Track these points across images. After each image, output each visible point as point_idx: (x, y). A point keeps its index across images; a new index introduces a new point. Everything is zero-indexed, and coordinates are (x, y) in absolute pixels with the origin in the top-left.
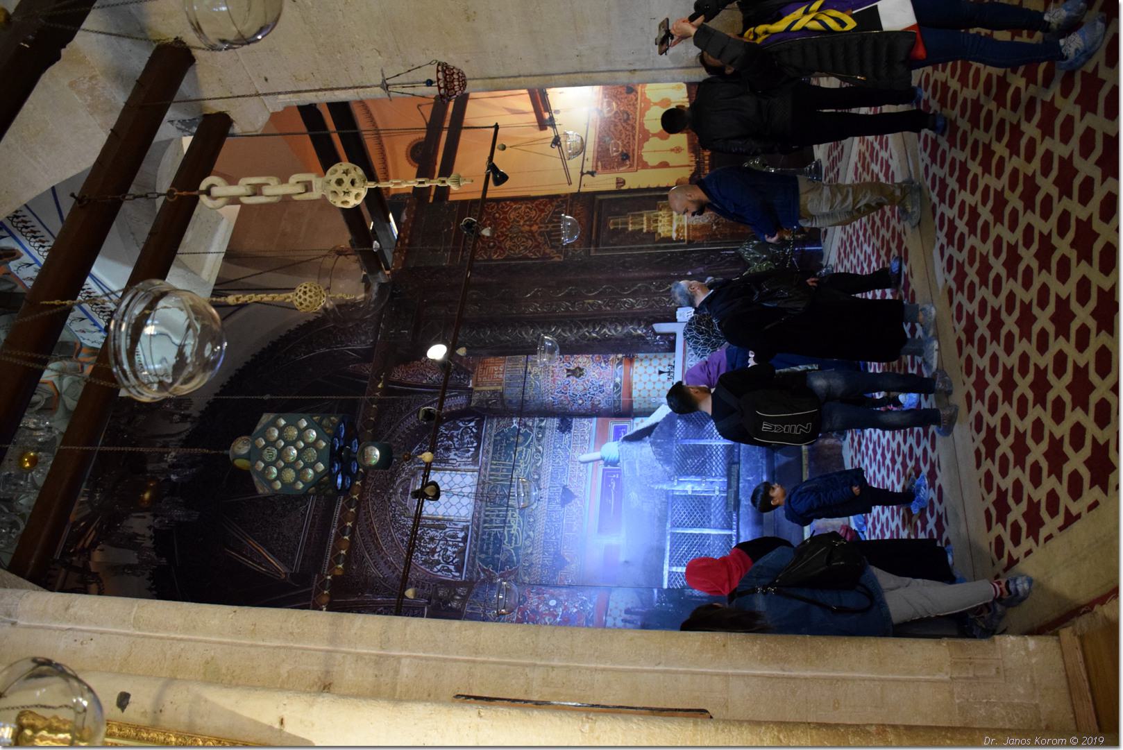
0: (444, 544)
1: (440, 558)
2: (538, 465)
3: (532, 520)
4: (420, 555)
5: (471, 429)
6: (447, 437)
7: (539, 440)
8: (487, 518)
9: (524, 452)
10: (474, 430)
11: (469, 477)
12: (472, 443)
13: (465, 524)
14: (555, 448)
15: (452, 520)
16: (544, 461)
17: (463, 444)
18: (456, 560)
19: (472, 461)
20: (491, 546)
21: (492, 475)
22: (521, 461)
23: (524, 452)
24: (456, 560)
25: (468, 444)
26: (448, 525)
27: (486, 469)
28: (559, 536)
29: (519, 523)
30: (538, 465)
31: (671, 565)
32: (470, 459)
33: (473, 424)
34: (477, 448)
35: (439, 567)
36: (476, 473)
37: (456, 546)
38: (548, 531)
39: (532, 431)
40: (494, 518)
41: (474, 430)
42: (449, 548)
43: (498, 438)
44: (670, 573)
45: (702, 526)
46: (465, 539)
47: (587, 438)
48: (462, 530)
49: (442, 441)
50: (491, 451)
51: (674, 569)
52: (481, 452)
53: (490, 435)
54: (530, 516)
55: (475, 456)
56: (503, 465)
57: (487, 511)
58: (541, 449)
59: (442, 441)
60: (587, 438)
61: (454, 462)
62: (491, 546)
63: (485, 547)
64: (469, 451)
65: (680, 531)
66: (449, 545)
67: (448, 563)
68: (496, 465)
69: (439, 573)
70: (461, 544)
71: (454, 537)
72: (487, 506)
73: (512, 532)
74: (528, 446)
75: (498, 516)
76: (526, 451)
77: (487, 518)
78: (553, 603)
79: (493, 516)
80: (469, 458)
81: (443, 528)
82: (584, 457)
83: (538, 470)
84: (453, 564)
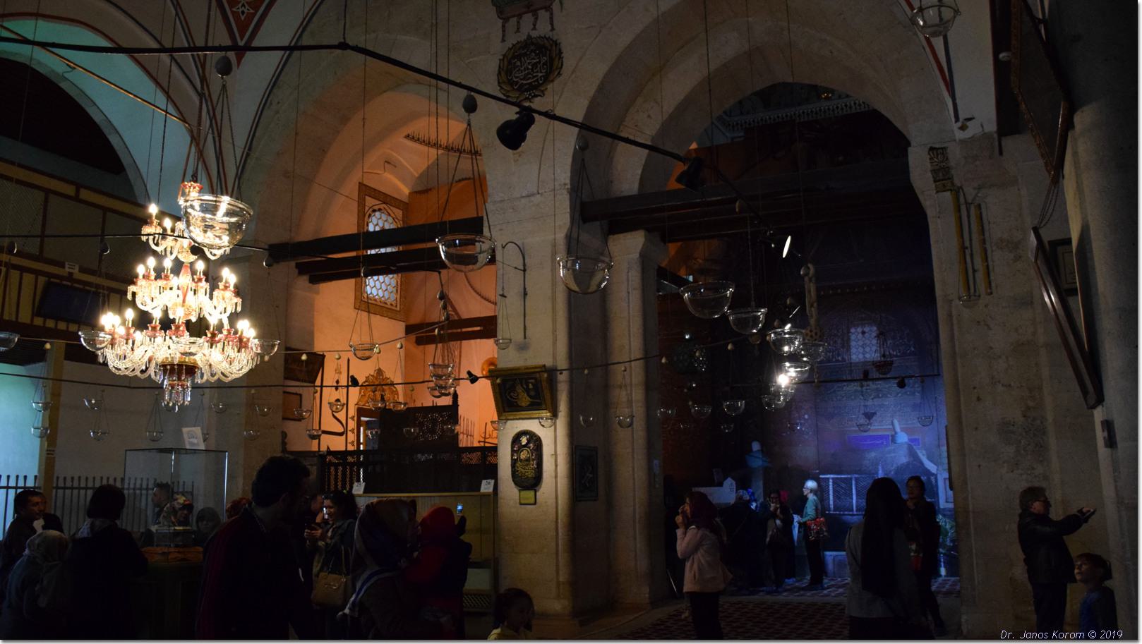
7: (906, 393)
30: (889, 395)
31: (833, 478)
33: (913, 349)
39: (912, 388)
41: (908, 352)
44: (828, 479)
45: (857, 495)
46: (838, 361)
48: (843, 358)
51: (831, 480)
65: (854, 482)
71: (839, 355)
78: (806, 417)
81: (843, 347)
82: (896, 422)
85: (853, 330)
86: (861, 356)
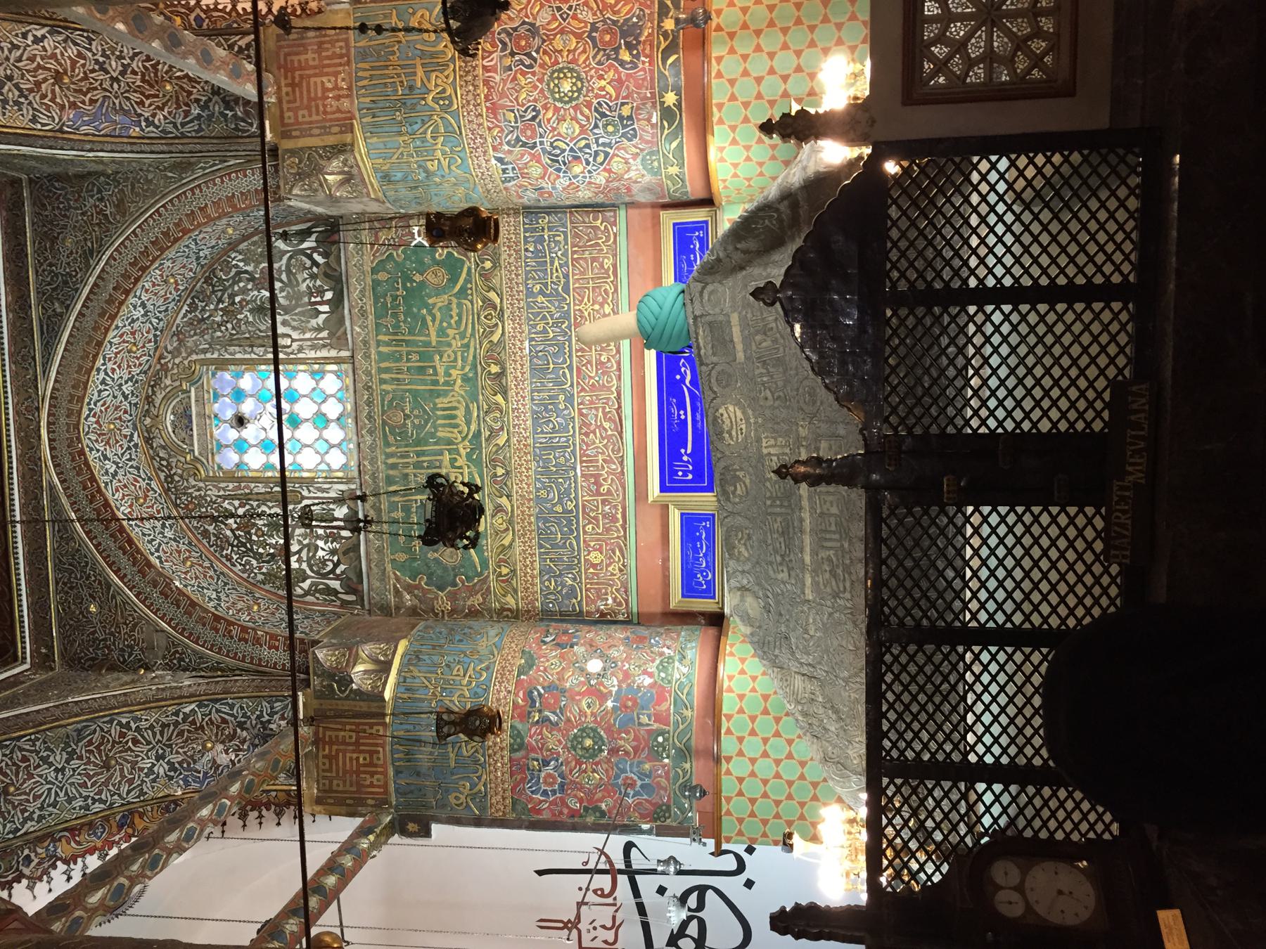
0: (305, 536)
1: (304, 566)
2: (495, 338)
3: (500, 471)
4: (254, 562)
5: (310, 257)
6: (252, 279)
7: (486, 276)
8: (391, 472)
9: (455, 312)
10: (319, 259)
11: (330, 378)
12: (321, 292)
13: (343, 487)
14: (530, 293)
15: (309, 482)
16: (508, 328)
17: (299, 296)
18: (342, 567)
19: (331, 335)
21: (387, 370)
22: (451, 332)
24: (342, 567)
25: (311, 294)
26: (305, 493)
27: (367, 356)
28: (570, 506)
30: (495, 338)
32: (325, 334)
33: (309, 244)
34: (337, 303)
35: (306, 585)
36: (344, 366)
37: (335, 538)
38: (543, 493)
40: (410, 470)
41: (319, 259)
42: (320, 543)
43: (382, 276)
47: (608, 263)
49: (244, 291)
50: (370, 308)
52: (346, 311)
53: (360, 267)
54: (494, 462)
55: (336, 323)
57: (389, 456)
58: (497, 301)
59: (244, 291)
60: (608, 263)
61: (288, 342)
66: (319, 537)
67: (325, 576)
68: (388, 344)
69: (309, 598)
70: (346, 533)
72: (388, 444)
74: (463, 292)
75: (418, 465)
76: (460, 305)
77: (391, 472)
79: (406, 465)
80: (319, 329)
83: (496, 353)
84: (337, 578)
85: (230, 459)
86: (334, 434)
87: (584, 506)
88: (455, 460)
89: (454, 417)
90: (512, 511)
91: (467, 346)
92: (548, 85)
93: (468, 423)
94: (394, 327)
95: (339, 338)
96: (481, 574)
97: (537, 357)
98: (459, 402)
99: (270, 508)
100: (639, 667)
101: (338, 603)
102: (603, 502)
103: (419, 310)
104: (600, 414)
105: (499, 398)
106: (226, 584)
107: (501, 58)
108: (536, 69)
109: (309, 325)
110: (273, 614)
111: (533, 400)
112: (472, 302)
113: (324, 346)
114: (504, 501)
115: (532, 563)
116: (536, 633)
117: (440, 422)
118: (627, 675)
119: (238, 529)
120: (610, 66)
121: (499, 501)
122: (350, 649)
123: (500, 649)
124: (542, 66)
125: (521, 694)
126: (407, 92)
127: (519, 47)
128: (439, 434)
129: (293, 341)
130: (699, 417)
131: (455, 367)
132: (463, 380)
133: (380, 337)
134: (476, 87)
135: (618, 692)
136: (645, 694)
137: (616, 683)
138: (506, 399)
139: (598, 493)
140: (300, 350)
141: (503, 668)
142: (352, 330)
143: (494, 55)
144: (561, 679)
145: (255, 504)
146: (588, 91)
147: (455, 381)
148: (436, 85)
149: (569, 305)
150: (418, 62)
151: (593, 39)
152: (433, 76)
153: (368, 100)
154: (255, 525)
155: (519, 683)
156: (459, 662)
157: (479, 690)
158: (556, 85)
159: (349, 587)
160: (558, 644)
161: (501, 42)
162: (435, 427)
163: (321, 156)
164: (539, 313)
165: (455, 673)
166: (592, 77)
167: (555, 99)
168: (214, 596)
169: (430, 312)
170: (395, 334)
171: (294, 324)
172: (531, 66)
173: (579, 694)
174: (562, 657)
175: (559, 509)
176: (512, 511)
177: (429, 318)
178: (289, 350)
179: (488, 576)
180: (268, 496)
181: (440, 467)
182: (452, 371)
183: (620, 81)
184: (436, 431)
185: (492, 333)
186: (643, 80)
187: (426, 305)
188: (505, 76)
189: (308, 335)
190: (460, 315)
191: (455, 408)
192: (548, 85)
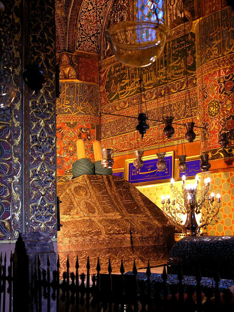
2: (172, 90)
9: (179, 71)
20: (118, 74)
23: (179, 71)
29: (132, 91)
30: (172, 90)
32: (175, 18)
56: (170, 55)
58: (183, 89)
62: (118, 74)
63: (117, 68)
64: (181, 13)
69: (105, 39)
73: (127, 88)
76: (181, 73)
80: (176, 15)
87: (126, 135)
88: (137, 83)
89: (149, 80)
90: (125, 108)
91: (170, 79)
92: (213, 101)
93: (148, 86)
94: (174, 47)
95: (173, 24)
96: (109, 101)
97: (167, 109)
98: (153, 80)
99: (126, 15)
100: (71, 163)
101: (104, 50)
102: (128, 142)
103: (180, 56)
104: (151, 137)
105: (155, 96)
106: (102, 9)
107: (223, 77)
108: (219, 94)
109: (178, 11)
110: (91, 30)
111: (154, 109)
112: (183, 77)
113: (171, 19)
114: (127, 105)
115: (112, 119)
116: (87, 125)
117: (147, 74)
118: (69, 159)
119: (121, 6)
120: (219, 127)
121: (127, 103)
122: (69, 64)
123: (80, 113)
124: (220, 97)
125: (60, 125)
126: (211, 38)
127: (227, 84)
128: (144, 75)
129: (173, 5)
130: (148, 176)
131: (163, 76)
132: (159, 80)
133: (171, 42)
134: (213, 68)
135: (62, 158)
136: (61, 166)
137: (65, 156)
138: (154, 99)
139: (130, 140)
140: (170, 10)
141: (69, 117)
142: (173, 30)
143: (224, 74)
144: (67, 137)
145: (127, 9)
146: (211, 119)
147: (159, 77)
148: (213, 50)
149: (183, 119)
150: (221, 40)
151: (229, 118)
152: (216, 48)
153: (208, 22)
154: (122, 11)
155: (64, 123)
156: (70, 102)
157: (61, 111)
158: (213, 104)
159: (108, 52)
160: (80, 134)
161: (229, 76)
162: (146, 73)
163: (190, 6)
164: (179, 106)
165: (66, 101)
166: (216, 120)
167: (209, 105)
168: (89, 9)
169: (179, 61)
170: (172, 49)
171: (178, 3)
172: (220, 92)
173: (61, 145)
174: (75, 136)
175: (126, 126)
176: (125, 108)
177: (177, 61)
178: (170, 5)
179: (109, 103)
180: (129, 13)
181: (135, 78)
182: (162, 75)
183: (215, 132)
184: (145, 73)
185: (173, 89)
186: (215, 143)
187: (181, 59)
188: (216, 81)
189: (174, 11)
190: (179, 74)
191: (151, 80)
192: (213, 101)
